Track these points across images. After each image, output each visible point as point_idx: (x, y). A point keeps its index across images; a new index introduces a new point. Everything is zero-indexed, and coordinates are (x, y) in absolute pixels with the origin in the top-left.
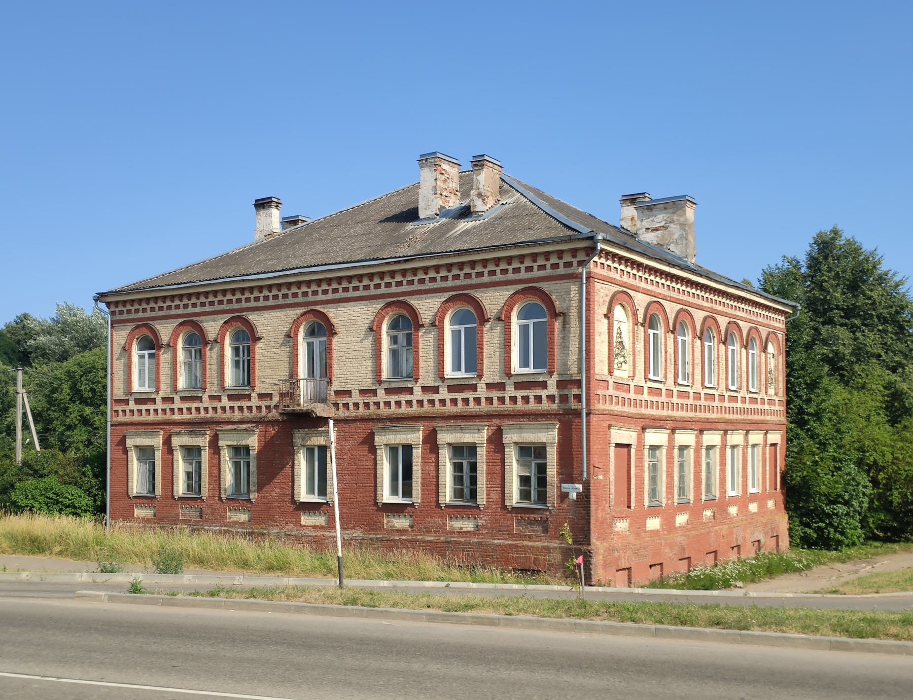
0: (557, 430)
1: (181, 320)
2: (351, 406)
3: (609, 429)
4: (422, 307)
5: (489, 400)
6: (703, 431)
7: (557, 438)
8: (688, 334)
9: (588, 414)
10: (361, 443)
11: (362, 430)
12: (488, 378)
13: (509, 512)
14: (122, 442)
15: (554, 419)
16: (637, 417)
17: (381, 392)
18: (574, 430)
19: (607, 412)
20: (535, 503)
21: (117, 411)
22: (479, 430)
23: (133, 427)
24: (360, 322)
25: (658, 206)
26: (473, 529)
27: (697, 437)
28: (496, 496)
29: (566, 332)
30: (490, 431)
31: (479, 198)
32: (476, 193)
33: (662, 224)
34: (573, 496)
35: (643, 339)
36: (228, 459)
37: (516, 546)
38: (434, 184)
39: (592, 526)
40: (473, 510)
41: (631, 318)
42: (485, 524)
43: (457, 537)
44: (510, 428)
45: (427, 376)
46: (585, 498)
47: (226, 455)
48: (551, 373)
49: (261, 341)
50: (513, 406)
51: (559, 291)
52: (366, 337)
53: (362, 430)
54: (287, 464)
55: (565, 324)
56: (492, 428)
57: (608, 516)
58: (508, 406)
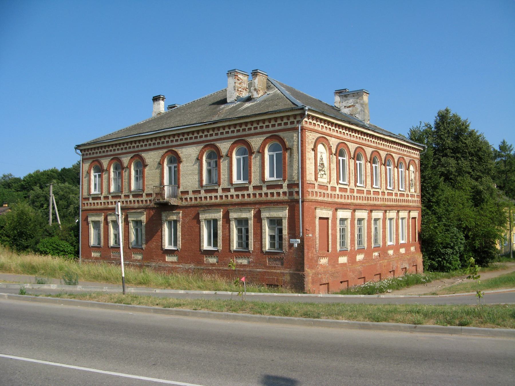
0: (287, 210)
1: (112, 157)
2: (189, 199)
3: (315, 210)
4: (222, 147)
5: (254, 195)
6: (372, 211)
7: (287, 215)
8: (363, 160)
9: (302, 202)
10: (193, 219)
11: (193, 211)
13: (264, 254)
14: (86, 219)
15: (286, 205)
16: (332, 203)
17: (203, 192)
18: (296, 210)
19: (314, 200)
20: (277, 249)
21: (84, 204)
22: (249, 211)
23: (91, 212)
24: (193, 155)
25: (350, 95)
26: (247, 263)
27: (368, 214)
28: (258, 246)
29: (292, 158)
30: (255, 211)
31: (255, 91)
32: (254, 89)
33: (352, 104)
34: (296, 245)
35: (335, 162)
36: (132, 227)
37: (268, 272)
38: (234, 85)
39: (305, 261)
40: (247, 253)
41: (328, 151)
42: (253, 261)
43: (239, 268)
44: (265, 209)
45: (224, 184)
46: (301, 246)
47: (131, 225)
48: (284, 180)
49: (148, 166)
50: (266, 198)
51: (288, 136)
52: (195, 163)
53: (193, 211)
54: (159, 230)
55: (291, 154)
56: (256, 210)
57: (315, 256)
58: (264, 198)
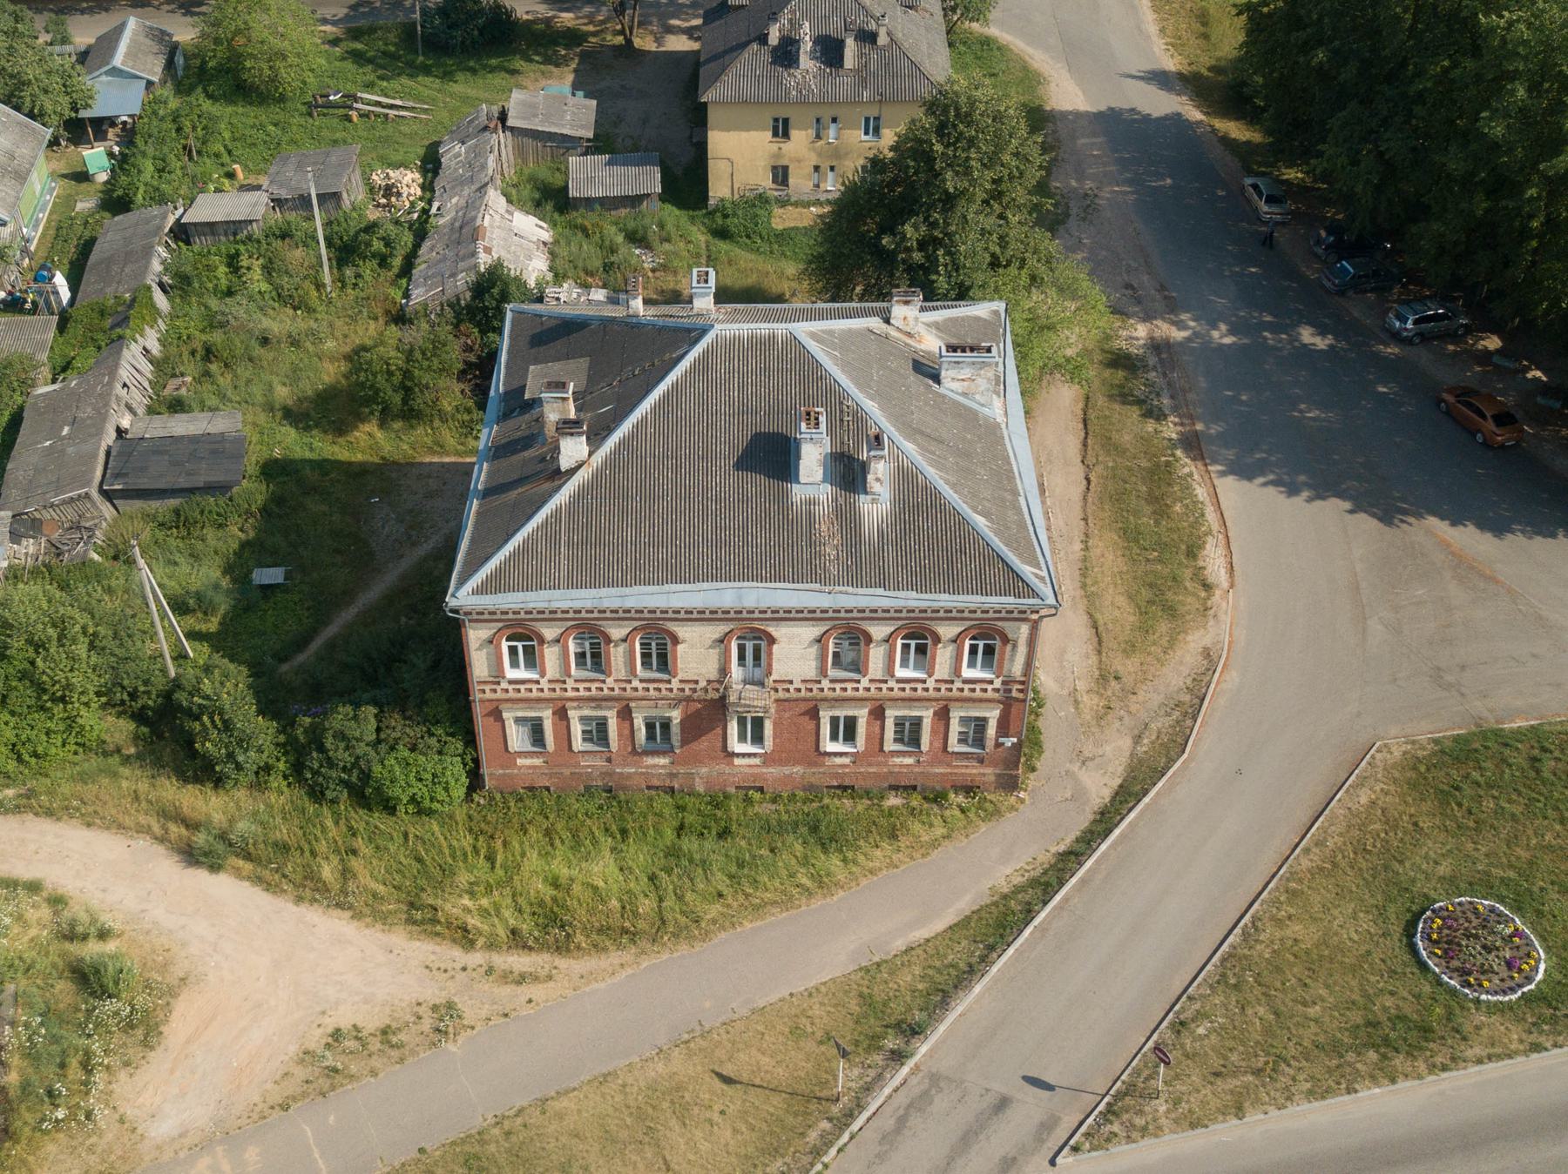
12: (937, 676)
14: (496, 714)
20: (972, 746)
28: (938, 744)
52: (810, 645)
